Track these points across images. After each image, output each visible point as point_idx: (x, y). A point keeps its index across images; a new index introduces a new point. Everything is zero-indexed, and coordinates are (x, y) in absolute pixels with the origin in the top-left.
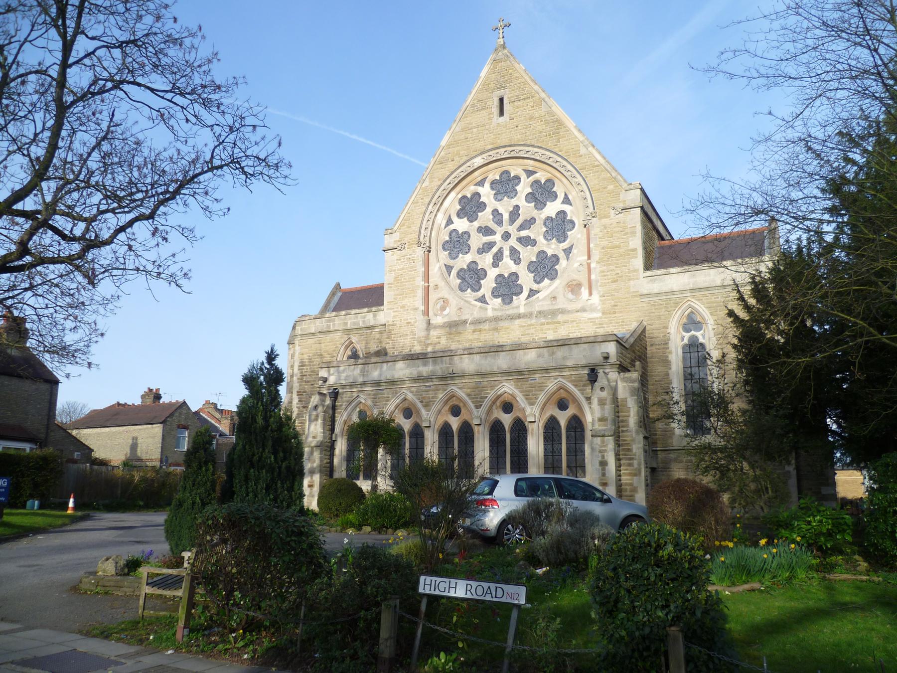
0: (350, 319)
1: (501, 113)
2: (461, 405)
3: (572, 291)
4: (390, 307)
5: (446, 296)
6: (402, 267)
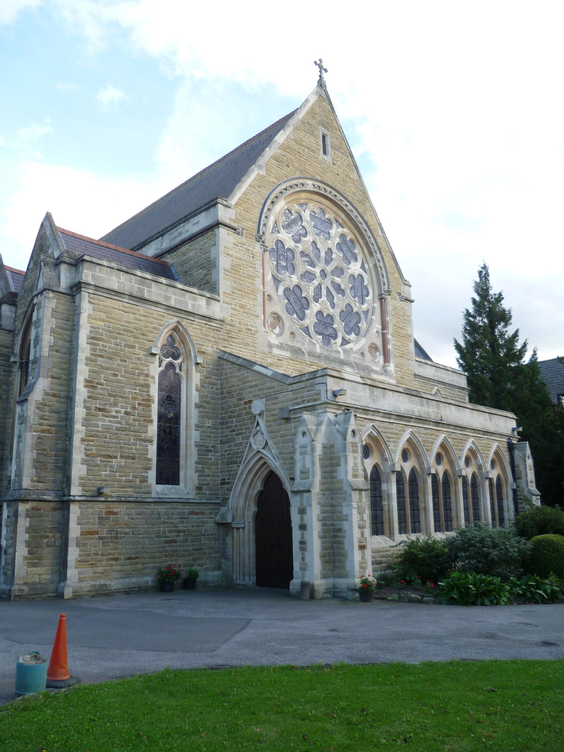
0: (175, 294)
1: (325, 152)
2: (443, 453)
3: (370, 352)
4: (227, 300)
5: (280, 313)
6: (239, 255)
